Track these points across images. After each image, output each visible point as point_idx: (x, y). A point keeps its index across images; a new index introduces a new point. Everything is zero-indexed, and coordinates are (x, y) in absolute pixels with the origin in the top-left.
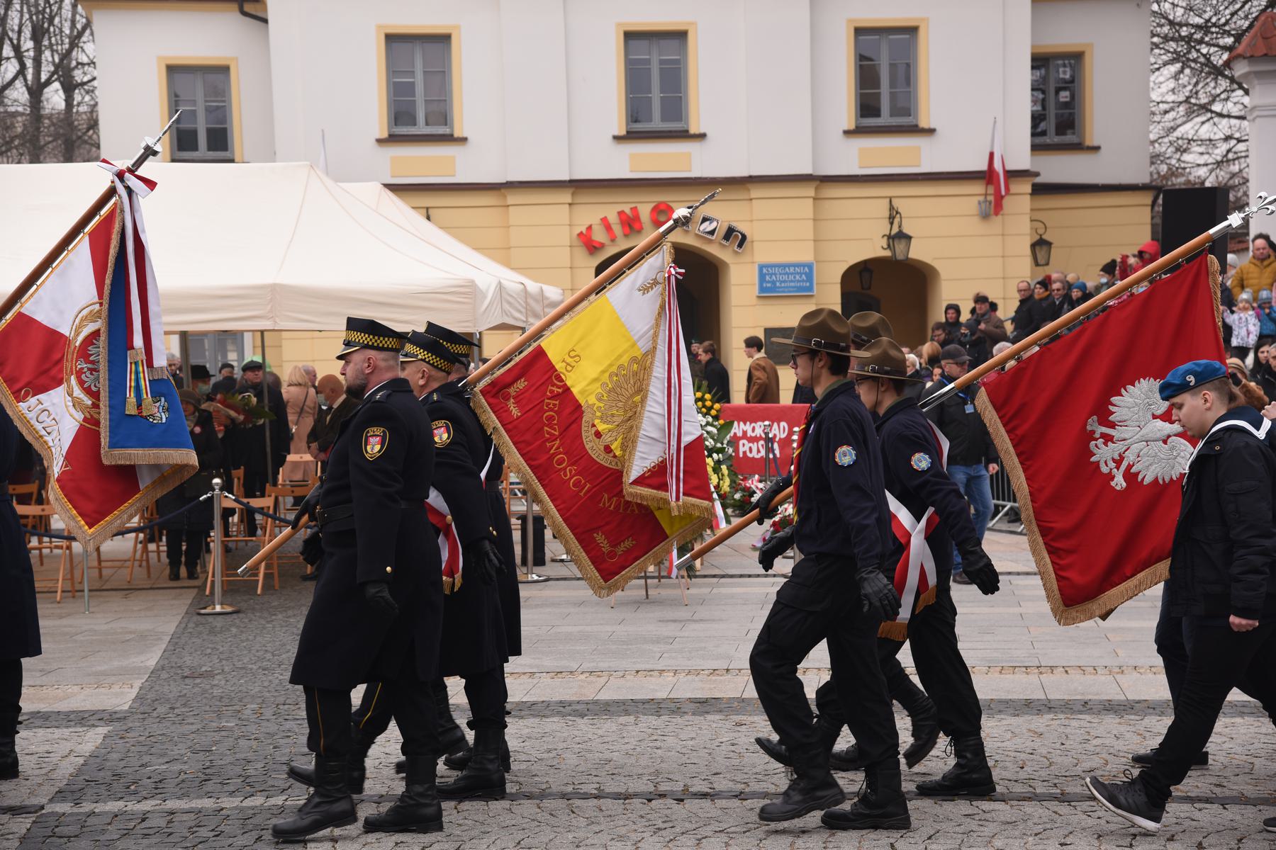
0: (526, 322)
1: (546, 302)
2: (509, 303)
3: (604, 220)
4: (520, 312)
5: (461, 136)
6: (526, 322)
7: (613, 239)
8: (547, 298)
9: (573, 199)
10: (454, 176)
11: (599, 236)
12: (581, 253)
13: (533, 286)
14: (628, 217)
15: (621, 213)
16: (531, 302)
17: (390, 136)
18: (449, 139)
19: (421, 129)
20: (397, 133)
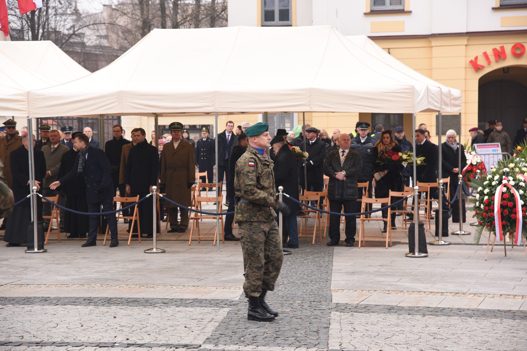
0: (441, 108)
1: (452, 97)
2: (432, 98)
3: (485, 54)
4: (437, 102)
5: (408, 10)
6: (441, 108)
7: (489, 62)
8: (452, 95)
9: (467, 43)
10: (404, 31)
11: (482, 62)
12: (471, 71)
13: (445, 89)
14: (499, 51)
15: (495, 50)
16: (443, 97)
17: (371, 11)
18: (402, 12)
19: (388, 7)
20: (375, 10)
